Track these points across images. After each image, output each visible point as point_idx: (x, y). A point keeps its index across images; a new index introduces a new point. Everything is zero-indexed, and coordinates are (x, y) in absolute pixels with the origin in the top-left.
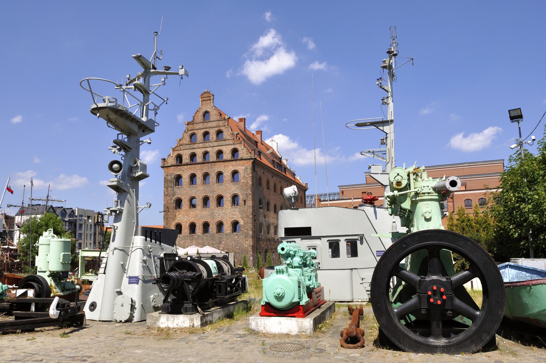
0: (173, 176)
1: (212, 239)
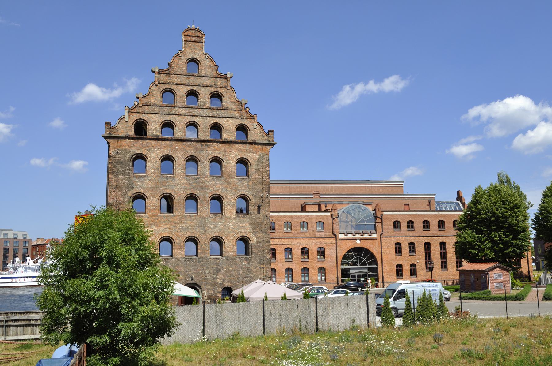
0: (128, 156)
1: (203, 266)
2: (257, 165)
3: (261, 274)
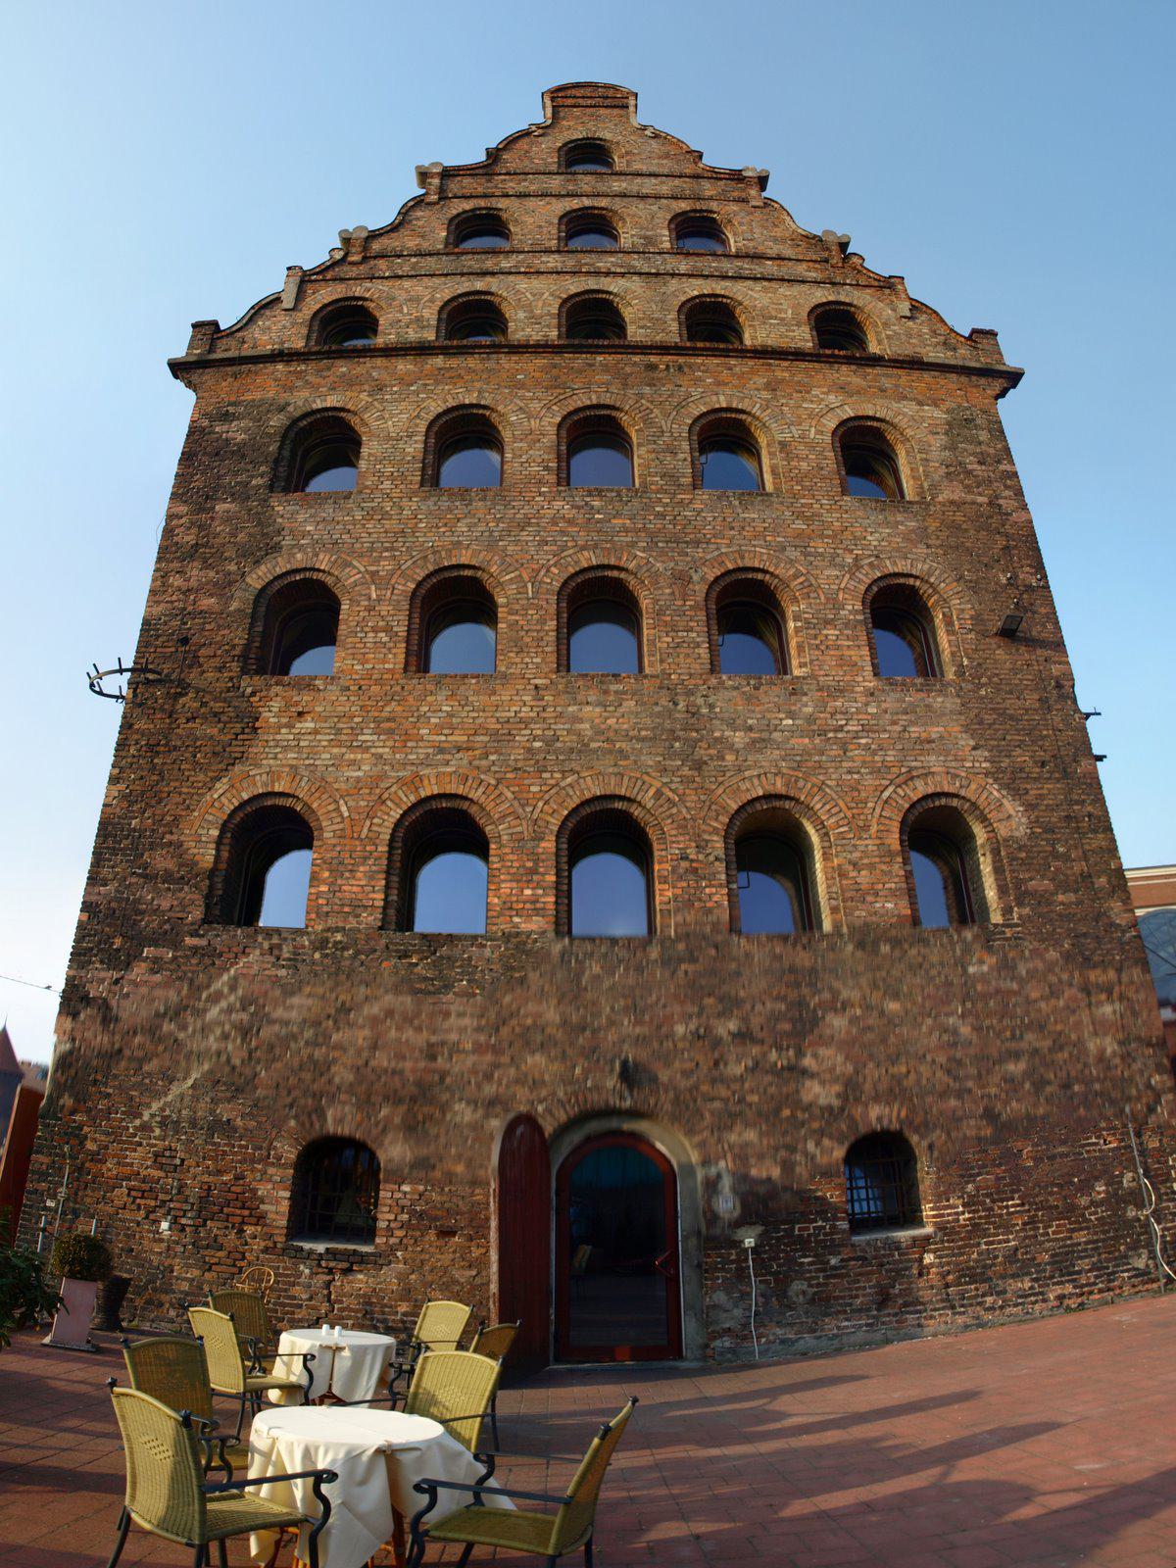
1: (695, 991)
2: (953, 448)
3: (1100, 1027)
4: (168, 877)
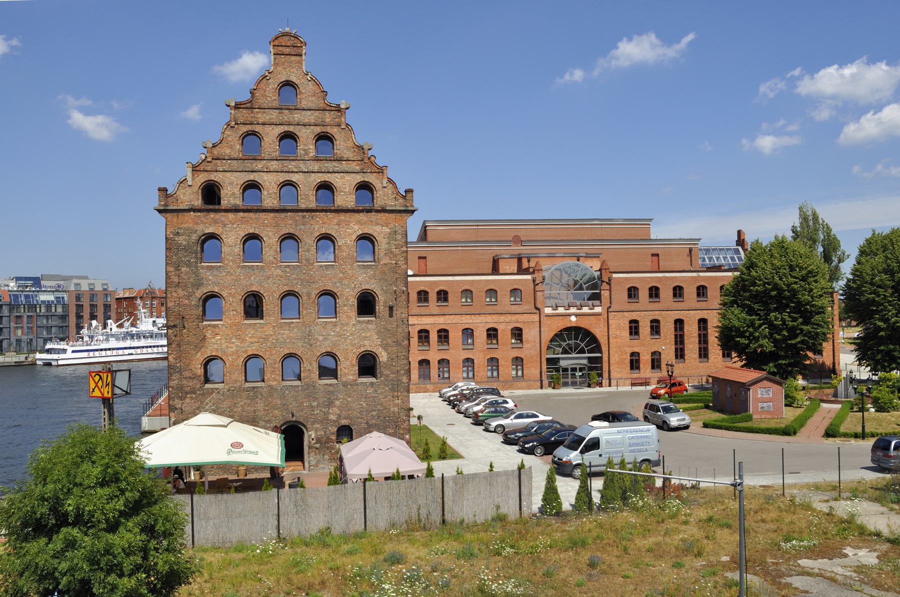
0: (194, 237)
2: (389, 243)
3: (395, 405)
4: (190, 378)
